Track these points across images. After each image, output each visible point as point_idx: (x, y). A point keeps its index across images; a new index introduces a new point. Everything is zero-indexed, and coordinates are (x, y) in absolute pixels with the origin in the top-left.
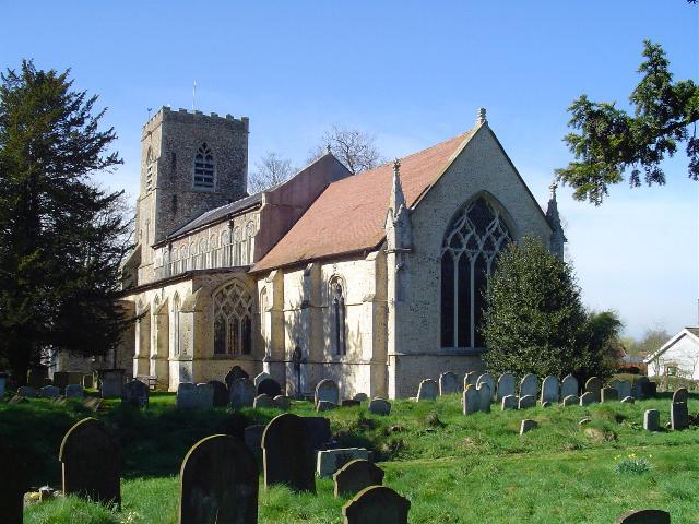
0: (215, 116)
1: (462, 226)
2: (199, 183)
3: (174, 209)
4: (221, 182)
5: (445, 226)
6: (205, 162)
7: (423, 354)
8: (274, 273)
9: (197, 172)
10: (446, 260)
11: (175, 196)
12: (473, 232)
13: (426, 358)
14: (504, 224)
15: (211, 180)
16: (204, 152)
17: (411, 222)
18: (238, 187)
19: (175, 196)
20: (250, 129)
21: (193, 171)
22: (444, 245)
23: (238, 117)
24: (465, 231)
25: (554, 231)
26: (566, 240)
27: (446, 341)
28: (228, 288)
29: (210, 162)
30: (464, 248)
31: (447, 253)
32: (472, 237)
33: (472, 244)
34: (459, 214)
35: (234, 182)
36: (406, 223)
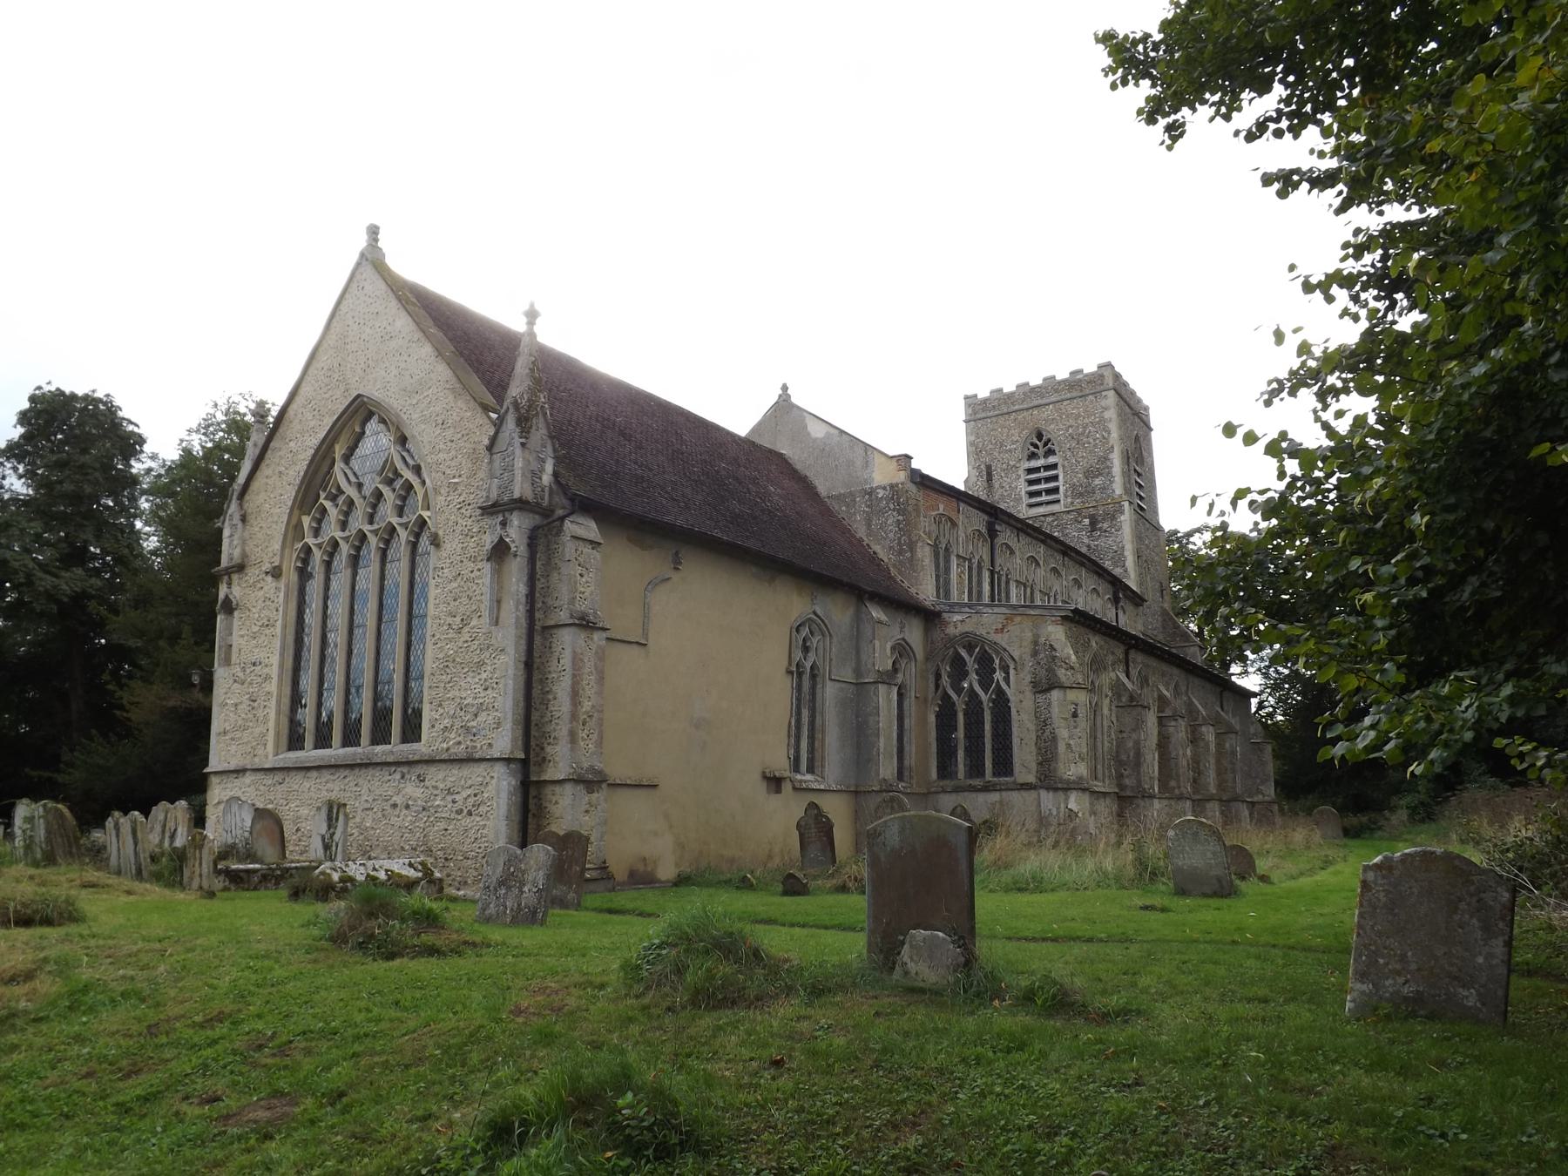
2: (1034, 500)
4: (1076, 492)
6: (1040, 462)
15: (1056, 490)
16: (1041, 443)
18: (1103, 489)
21: (1023, 488)
29: (1052, 460)
35: (1097, 482)
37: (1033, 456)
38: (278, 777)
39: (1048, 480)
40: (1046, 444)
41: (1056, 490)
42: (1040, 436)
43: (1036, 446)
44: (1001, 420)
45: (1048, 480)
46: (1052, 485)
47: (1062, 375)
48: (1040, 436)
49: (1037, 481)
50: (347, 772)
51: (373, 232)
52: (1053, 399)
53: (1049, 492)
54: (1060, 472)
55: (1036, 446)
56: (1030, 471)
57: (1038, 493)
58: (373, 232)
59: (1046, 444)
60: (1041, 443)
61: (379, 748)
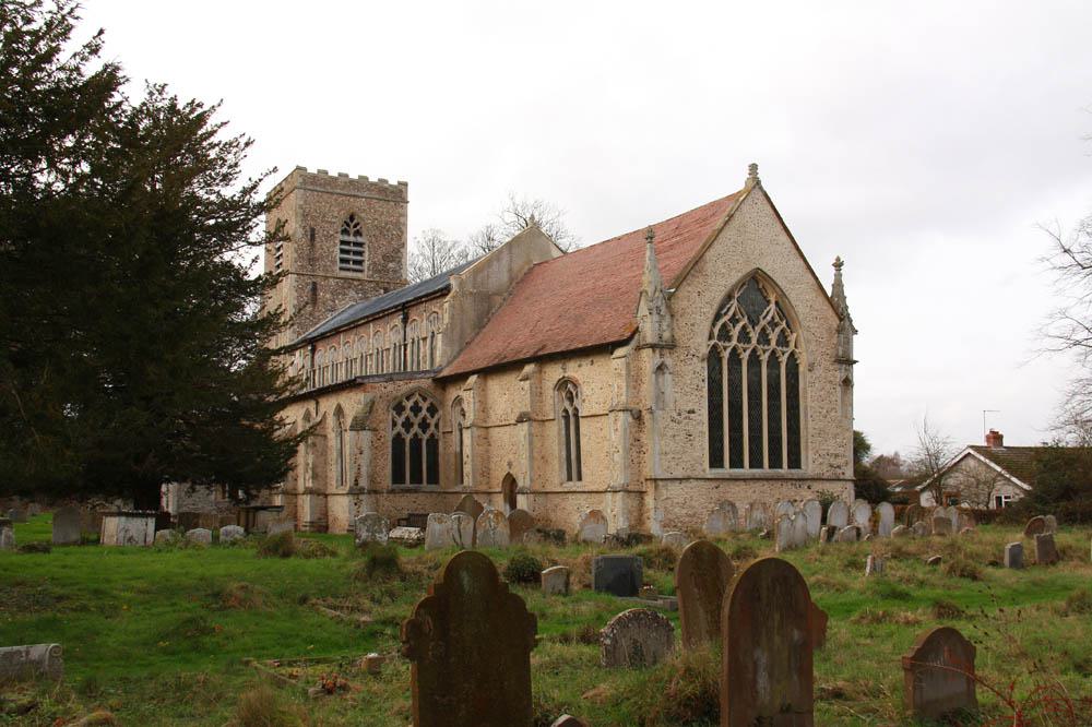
0: (363, 179)
1: (731, 313)
2: (344, 265)
3: (314, 300)
4: (375, 268)
5: (711, 313)
6: (352, 238)
7: (688, 479)
8: (473, 379)
9: (342, 251)
10: (714, 357)
11: (314, 284)
12: (745, 321)
13: (694, 483)
14: (783, 312)
15: (360, 263)
16: (351, 224)
17: (669, 307)
18: (395, 271)
19: (314, 284)
20: (410, 197)
22: (710, 338)
23: (393, 182)
24: (734, 320)
25: (841, 320)
26: (856, 332)
27: (716, 461)
28: (408, 398)
29: (360, 239)
30: (734, 342)
31: (715, 347)
32: (744, 327)
33: (744, 336)
34: (729, 297)
35: (391, 265)
36: (663, 309)
37: (345, 232)
38: (714, 484)
39: (356, 253)
40: (355, 226)
41: (360, 263)
42: (352, 218)
43: (348, 225)
44: (325, 196)
45: (356, 253)
46: (359, 258)
47: (373, 179)
48: (352, 218)
49: (348, 252)
50: (765, 483)
51: (754, 168)
52: (365, 194)
53: (355, 262)
54: (366, 249)
55: (348, 225)
56: (342, 242)
57: (347, 261)
58: (754, 168)
59: (355, 226)
60: (351, 224)
61: (793, 471)
